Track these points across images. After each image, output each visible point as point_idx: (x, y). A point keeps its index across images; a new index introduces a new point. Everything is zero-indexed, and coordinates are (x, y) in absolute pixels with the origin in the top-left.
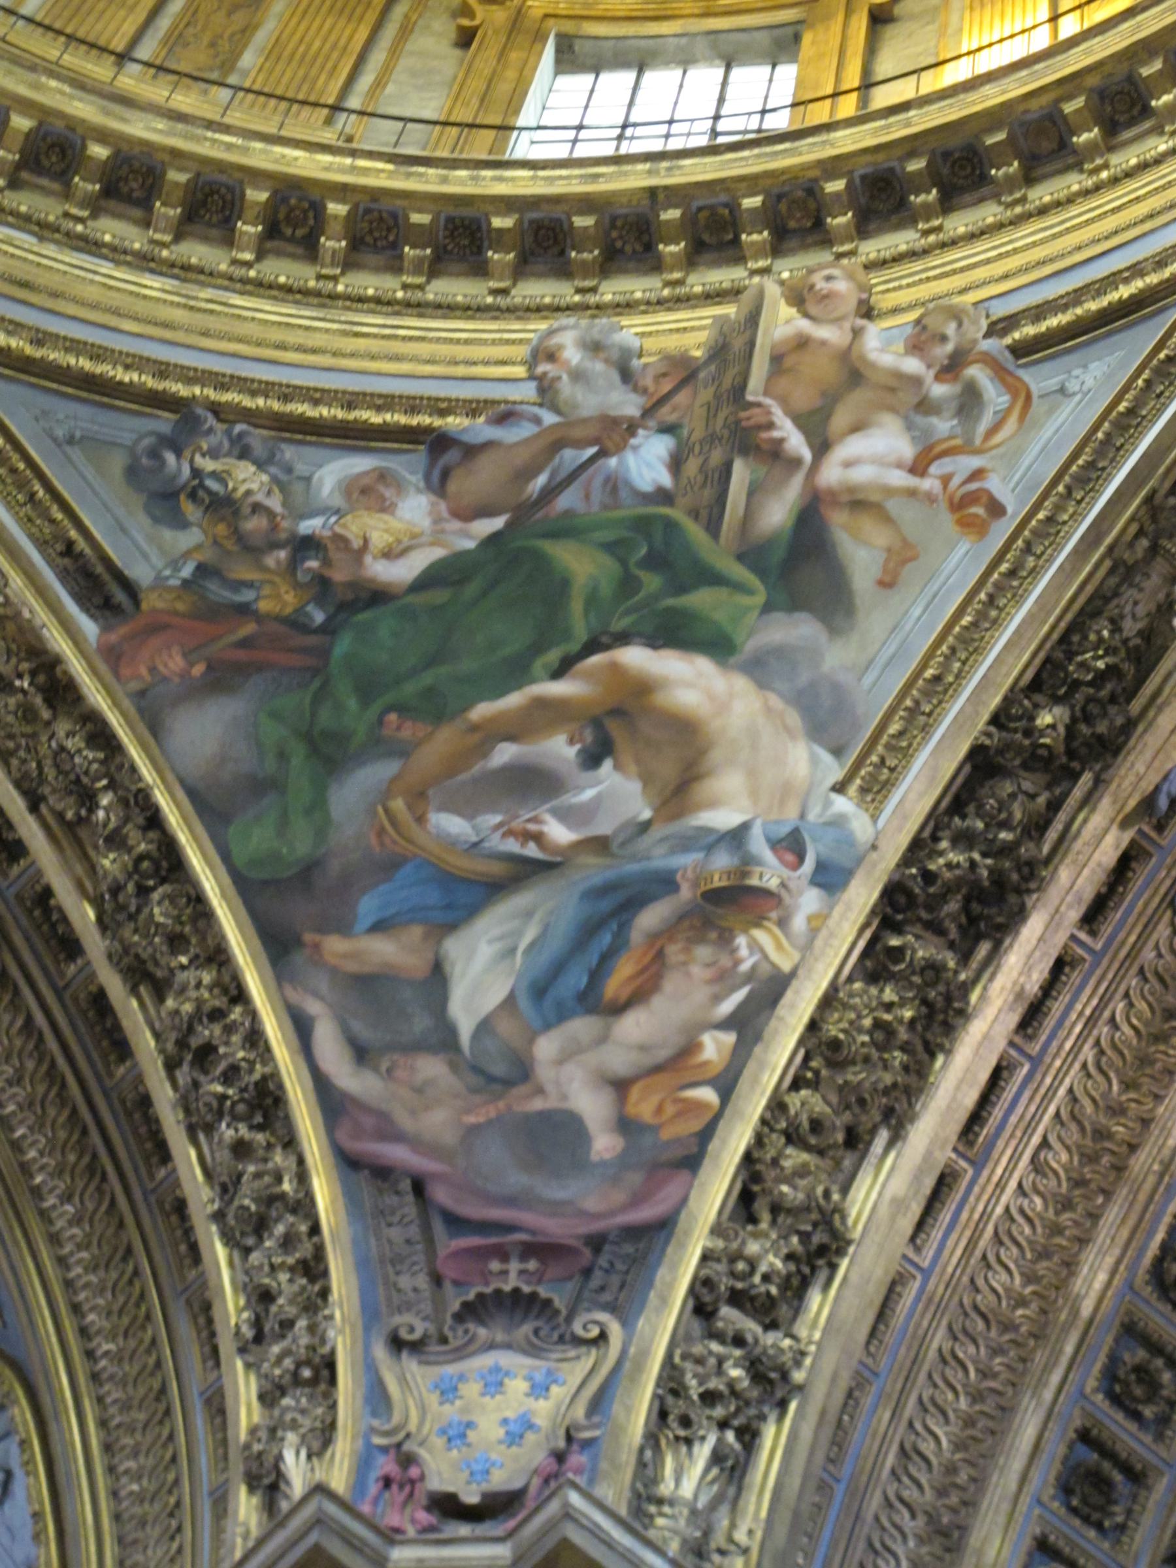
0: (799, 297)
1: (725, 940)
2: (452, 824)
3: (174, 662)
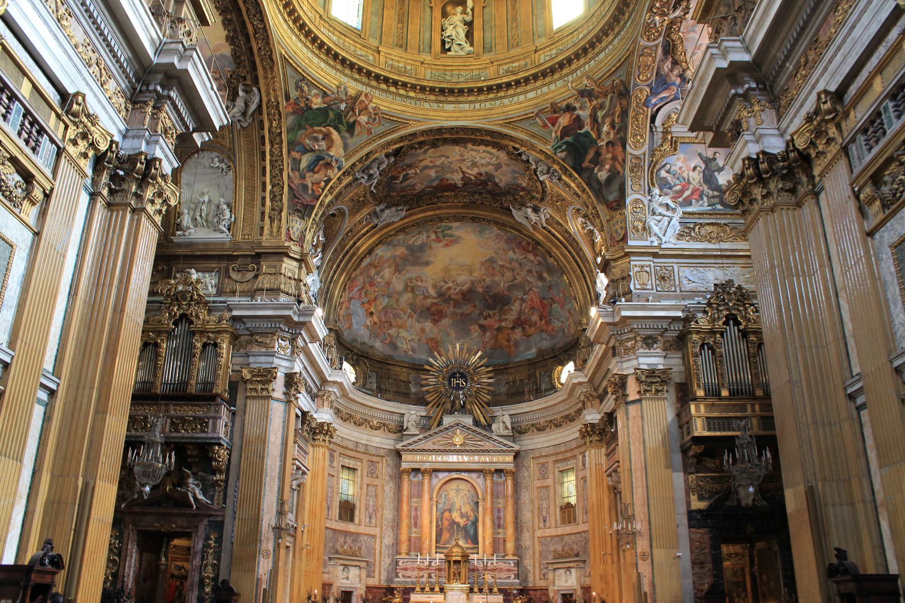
0: (366, 95)
1: (327, 170)
2: (307, 141)
3: (290, 109)
